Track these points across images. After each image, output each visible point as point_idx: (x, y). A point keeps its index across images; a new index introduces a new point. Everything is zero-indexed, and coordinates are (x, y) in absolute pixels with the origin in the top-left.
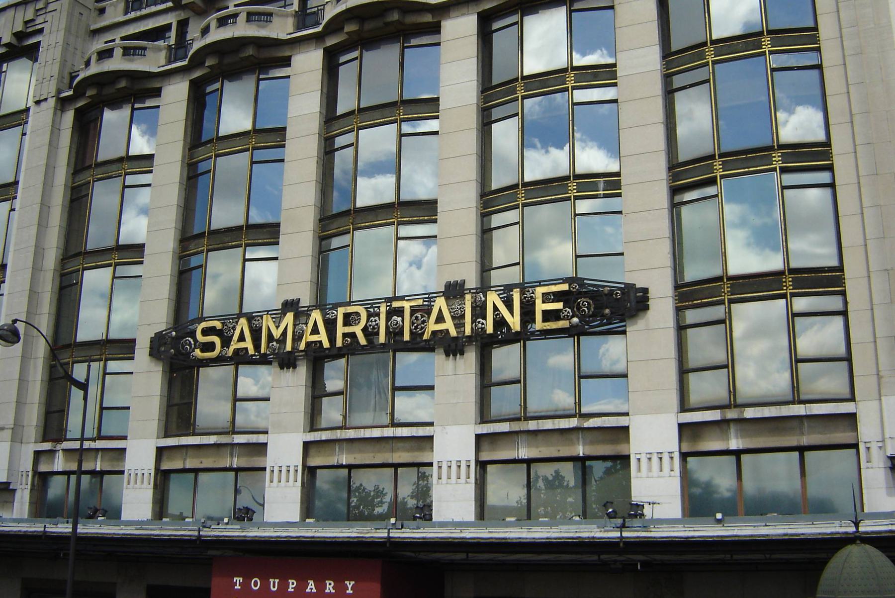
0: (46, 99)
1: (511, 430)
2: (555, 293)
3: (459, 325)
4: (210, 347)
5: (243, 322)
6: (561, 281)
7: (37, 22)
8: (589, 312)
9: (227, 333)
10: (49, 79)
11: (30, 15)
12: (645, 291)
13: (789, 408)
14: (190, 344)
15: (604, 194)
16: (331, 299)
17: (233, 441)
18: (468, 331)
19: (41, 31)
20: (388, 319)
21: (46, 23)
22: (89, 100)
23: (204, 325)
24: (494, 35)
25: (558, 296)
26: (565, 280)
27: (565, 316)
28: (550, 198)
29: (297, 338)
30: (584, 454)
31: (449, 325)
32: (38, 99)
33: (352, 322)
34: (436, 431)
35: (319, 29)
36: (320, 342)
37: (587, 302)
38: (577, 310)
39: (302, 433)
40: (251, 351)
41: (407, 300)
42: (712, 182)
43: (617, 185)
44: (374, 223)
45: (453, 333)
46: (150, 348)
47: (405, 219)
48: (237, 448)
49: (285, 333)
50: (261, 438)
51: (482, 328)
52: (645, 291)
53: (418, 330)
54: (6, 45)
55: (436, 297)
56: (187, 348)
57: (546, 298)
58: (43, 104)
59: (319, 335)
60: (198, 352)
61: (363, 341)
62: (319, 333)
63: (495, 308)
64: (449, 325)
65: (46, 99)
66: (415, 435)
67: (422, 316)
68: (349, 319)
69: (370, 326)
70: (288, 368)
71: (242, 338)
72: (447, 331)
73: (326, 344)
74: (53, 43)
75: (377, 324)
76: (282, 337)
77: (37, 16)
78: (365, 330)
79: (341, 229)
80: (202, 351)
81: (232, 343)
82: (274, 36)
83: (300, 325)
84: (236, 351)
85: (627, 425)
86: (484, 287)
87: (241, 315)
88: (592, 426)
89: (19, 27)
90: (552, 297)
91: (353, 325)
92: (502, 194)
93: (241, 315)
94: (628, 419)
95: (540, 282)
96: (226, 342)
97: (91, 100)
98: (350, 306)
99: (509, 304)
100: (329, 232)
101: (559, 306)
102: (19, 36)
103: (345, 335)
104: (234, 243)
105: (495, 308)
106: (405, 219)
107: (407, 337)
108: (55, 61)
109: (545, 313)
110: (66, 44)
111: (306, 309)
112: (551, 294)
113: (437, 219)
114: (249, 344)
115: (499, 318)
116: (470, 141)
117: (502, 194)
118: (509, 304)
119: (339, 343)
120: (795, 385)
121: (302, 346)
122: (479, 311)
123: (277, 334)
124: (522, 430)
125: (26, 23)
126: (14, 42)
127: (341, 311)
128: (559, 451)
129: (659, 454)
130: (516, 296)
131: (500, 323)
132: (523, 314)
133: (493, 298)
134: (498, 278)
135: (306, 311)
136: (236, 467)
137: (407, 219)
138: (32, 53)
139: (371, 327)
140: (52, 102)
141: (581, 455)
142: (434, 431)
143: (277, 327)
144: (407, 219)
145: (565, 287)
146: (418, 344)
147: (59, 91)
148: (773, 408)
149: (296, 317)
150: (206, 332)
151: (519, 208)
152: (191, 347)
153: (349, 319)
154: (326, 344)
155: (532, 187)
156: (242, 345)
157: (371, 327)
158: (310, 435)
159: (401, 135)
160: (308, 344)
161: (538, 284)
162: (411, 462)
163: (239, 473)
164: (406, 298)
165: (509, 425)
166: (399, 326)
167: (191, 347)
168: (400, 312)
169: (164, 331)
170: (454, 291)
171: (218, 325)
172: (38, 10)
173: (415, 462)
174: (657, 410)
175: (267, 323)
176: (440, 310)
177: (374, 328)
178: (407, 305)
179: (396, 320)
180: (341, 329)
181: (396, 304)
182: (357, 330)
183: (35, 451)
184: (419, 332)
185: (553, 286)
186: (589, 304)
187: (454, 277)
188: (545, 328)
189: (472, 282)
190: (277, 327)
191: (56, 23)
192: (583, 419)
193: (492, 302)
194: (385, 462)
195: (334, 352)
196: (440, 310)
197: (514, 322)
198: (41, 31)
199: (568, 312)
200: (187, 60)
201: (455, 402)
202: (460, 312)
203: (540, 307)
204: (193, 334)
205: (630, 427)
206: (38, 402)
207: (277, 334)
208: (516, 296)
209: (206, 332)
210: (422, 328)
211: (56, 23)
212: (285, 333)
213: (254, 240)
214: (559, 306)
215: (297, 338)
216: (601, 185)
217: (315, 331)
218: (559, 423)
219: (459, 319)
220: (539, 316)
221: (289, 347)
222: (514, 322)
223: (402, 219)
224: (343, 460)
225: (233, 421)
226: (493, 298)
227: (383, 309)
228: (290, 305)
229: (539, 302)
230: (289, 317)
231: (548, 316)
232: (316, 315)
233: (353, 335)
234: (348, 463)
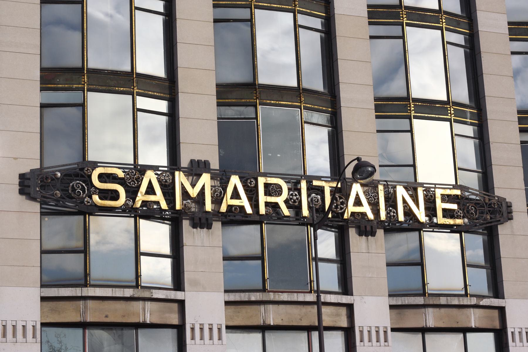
1: (425, 304)
2: (449, 196)
3: (376, 212)
4: (115, 195)
6: (452, 187)
8: (476, 215)
9: (130, 183)
13: (102, 295)
14: (83, 189)
15: (471, 122)
17: (152, 296)
18: (383, 216)
20: (309, 196)
27: (458, 215)
28: (435, 116)
29: (217, 200)
30: (475, 326)
33: (273, 193)
34: (506, 301)
36: (158, 203)
37: (473, 206)
39: (506, 300)
41: (325, 181)
44: (280, 102)
45: (371, 216)
46: (20, 185)
47: (308, 106)
48: (91, 303)
49: (202, 192)
51: (394, 216)
53: (338, 209)
55: (435, 188)
56: (79, 192)
57: (447, 198)
59: (240, 201)
60: (96, 198)
61: (286, 211)
62: (240, 199)
63: (404, 201)
64: (366, 209)
66: (340, 302)
67: (340, 198)
69: (291, 199)
70: (202, 227)
71: (150, 190)
72: (364, 214)
73: (249, 210)
75: (297, 199)
76: (378, 208)
78: (286, 202)
79: (243, 100)
80: (101, 198)
81: (139, 194)
83: (217, 187)
84: (145, 203)
85: (504, 306)
88: (484, 304)
90: (447, 199)
91: (273, 196)
92: (392, 103)
94: (504, 301)
95: (435, 184)
96: (132, 193)
100: (227, 100)
101: (454, 207)
103: (267, 204)
104: (122, 89)
105: (404, 201)
106: (308, 106)
109: (444, 210)
112: (446, 196)
114: (159, 196)
115: (407, 209)
117: (392, 103)
119: (262, 210)
121: (223, 208)
122: (391, 201)
123: (194, 192)
124: (435, 303)
128: (458, 323)
129: (526, 329)
131: (408, 213)
132: (427, 209)
136: (149, 323)
137: (310, 106)
139: (292, 200)
141: (473, 327)
142: (354, 300)
143: (193, 185)
144: (310, 106)
145: (458, 192)
148: (237, 294)
150: (102, 178)
152: (84, 192)
153: (271, 190)
154: (249, 210)
155: (420, 104)
156: (152, 198)
157: (292, 200)
158: (235, 296)
160: (230, 207)
161: (437, 186)
162: (333, 326)
163: (175, 331)
164: (322, 179)
165: (423, 299)
166: (319, 203)
167: (84, 192)
171: (120, 174)
173: (335, 326)
176: (357, 195)
177: (295, 202)
179: (317, 198)
180: (262, 199)
181: (315, 183)
182: (280, 200)
184: (340, 211)
185: (449, 190)
186: (475, 208)
188: (445, 223)
190: (193, 185)
192: (480, 299)
193: (356, 193)
194: (312, 325)
195: (257, 218)
196: (357, 195)
197: (421, 216)
199: (461, 213)
201: (370, 276)
202: (373, 200)
203: (440, 205)
205: (506, 307)
207: (194, 192)
210: (341, 209)
212: (202, 192)
213: (144, 90)
214: (454, 207)
215: (217, 200)
216: (468, 114)
217: (236, 195)
218: (463, 300)
219: (375, 206)
220: (440, 213)
222: (421, 216)
223: (307, 105)
224: (270, 321)
225: (138, 276)
227: (304, 185)
229: (438, 201)
230: (205, 179)
231: (447, 213)
232: (235, 180)
233: (275, 206)
234: (275, 324)
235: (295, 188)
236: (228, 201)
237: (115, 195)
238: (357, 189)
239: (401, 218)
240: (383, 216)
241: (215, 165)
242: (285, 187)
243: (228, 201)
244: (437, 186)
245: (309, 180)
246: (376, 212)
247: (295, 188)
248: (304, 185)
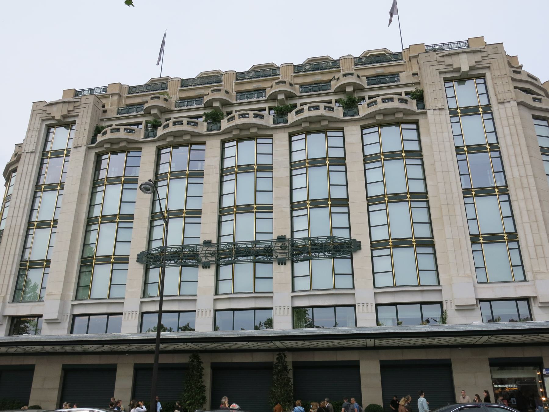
0: (81, 147)
7: (75, 111)
10: (33, 143)
11: (71, 108)
12: (360, 242)
19: (77, 116)
21: (80, 113)
22: (105, 149)
24: (225, 149)
32: (32, 151)
35: (156, 138)
52: (360, 242)
54: (57, 120)
58: (79, 149)
65: (81, 147)
74: (84, 121)
77: (75, 109)
82: (199, 132)
89: (65, 113)
95: (318, 237)
97: (233, 136)
98: (251, 241)
102: (64, 117)
108: (85, 130)
111: (215, 244)
113: (201, 216)
125: (69, 111)
126: (62, 119)
135: (215, 245)
138: (69, 125)
140: (84, 149)
151: (254, 212)
161: (318, 238)
169: (145, 251)
172: (75, 107)
183: (140, 302)
191: (85, 113)
198: (77, 116)
200: (95, 144)
206: (74, 282)
211: (85, 113)
244: (318, 238)
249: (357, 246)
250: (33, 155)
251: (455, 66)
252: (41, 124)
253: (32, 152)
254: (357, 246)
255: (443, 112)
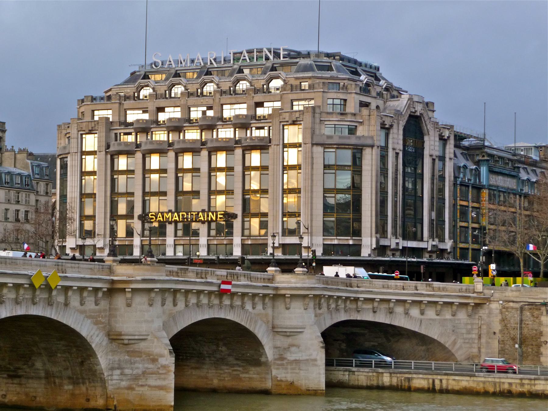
3: (204, 218)
4: (153, 219)
5: (160, 213)
11: (93, 126)
16: (178, 211)
18: (206, 219)
23: (151, 214)
25: (222, 214)
26: (223, 211)
29: (172, 218)
31: (202, 218)
38: (225, 218)
40: (162, 220)
42: (249, 195)
43: (233, 193)
45: (203, 220)
50: (165, 238)
57: (220, 214)
68: (182, 215)
71: (160, 217)
86: (209, 211)
87: (159, 212)
89: (91, 129)
93: (159, 212)
96: (156, 218)
99: (213, 215)
107: (194, 220)
110: (106, 136)
116: (206, 180)
118: (213, 215)
120: (260, 233)
121: (173, 220)
122: (208, 216)
123: (167, 217)
127: (181, 213)
130: (215, 214)
131: (211, 218)
133: (210, 214)
134: (212, 209)
140: (104, 152)
145: (223, 213)
146: (196, 221)
147: (106, 149)
149: (172, 213)
150: (151, 215)
156: (160, 219)
159: (192, 176)
160: (174, 220)
168: (193, 215)
170: (203, 211)
171: (154, 214)
174: (238, 236)
175: (165, 215)
178: (194, 213)
181: (192, 213)
187: (204, 208)
189: (207, 210)
197: (214, 218)
203: (219, 216)
204: (148, 216)
207: (167, 217)
208: (215, 214)
209: (151, 215)
215: (172, 218)
217: (176, 217)
219: (204, 217)
221: (170, 220)
222: (214, 218)
226: (210, 214)
227: (189, 214)
228: (170, 211)
230: (170, 214)
231: (220, 218)
232: (176, 214)
235: (187, 214)
236: (174, 218)
237: (153, 219)
238: (201, 214)
239: (210, 220)
240: (206, 219)
241: (173, 210)
242: (186, 214)
243: (174, 218)
245: (191, 212)
246: (204, 218)
247: (187, 214)
248: (189, 214)
249: (235, 216)
250: (76, 154)
251: (287, 120)
252: (78, 134)
253: (75, 153)
254: (235, 216)
255: (278, 147)
